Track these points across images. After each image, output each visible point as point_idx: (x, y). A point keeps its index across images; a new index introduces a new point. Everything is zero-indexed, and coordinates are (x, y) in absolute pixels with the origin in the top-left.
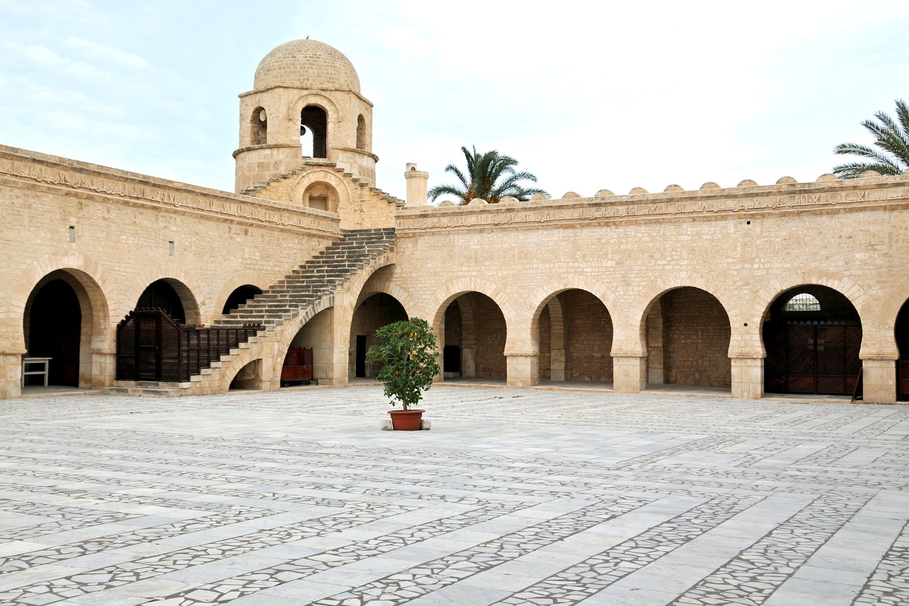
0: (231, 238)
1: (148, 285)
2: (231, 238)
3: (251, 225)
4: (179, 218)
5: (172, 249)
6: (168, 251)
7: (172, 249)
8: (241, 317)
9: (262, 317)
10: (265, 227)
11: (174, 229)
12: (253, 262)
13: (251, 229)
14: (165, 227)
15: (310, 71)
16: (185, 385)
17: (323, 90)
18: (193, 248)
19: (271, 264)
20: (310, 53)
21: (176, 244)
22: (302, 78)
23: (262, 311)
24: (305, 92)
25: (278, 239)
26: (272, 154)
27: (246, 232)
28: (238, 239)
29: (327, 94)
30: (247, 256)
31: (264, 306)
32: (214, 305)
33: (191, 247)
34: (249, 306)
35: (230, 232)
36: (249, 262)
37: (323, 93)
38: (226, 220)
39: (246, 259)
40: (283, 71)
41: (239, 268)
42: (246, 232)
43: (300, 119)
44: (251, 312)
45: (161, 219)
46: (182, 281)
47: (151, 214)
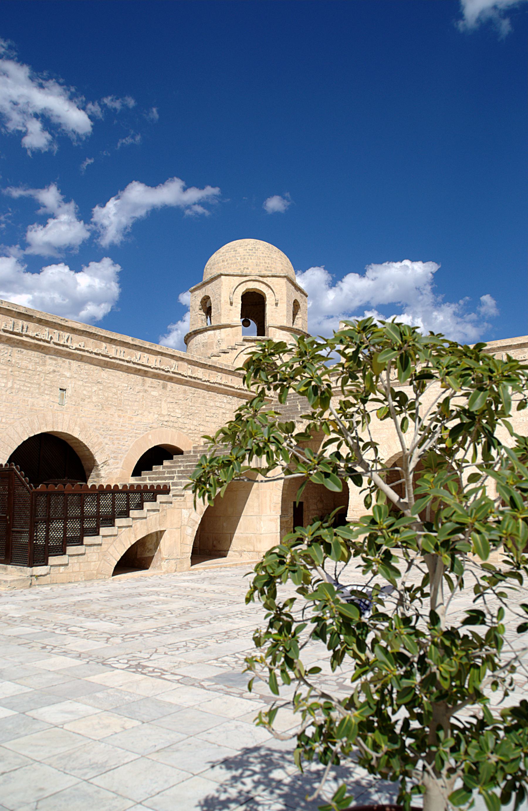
0: (146, 391)
1: (26, 438)
2: (146, 391)
3: (171, 379)
4: (75, 364)
5: (62, 397)
6: (58, 400)
7: (62, 397)
8: (150, 479)
9: (172, 478)
10: (187, 382)
11: (68, 374)
12: (172, 419)
13: (170, 384)
14: (54, 371)
15: (249, 261)
16: (39, 570)
17: (262, 276)
18: (94, 399)
19: (195, 423)
20: (249, 247)
21: (69, 393)
22: (242, 268)
23: (173, 472)
24: (245, 279)
25: (204, 397)
26: (215, 334)
27: (164, 387)
28: (155, 393)
29: (264, 280)
30: (165, 412)
31: (180, 466)
32: (120, 465)
33: (90, 397)
34: (164, 468)
35: (143, 385)
36: (166, 418)
37: (261, 279)
38: (137, 372)
39: (164, 416)
40: (226, 263)
41: (155, 425)
42: (164, 387)
43: (241, 302)
44: (164, 473)
45: (49, 361)
46: (76, 435)
47: (34, 355)
